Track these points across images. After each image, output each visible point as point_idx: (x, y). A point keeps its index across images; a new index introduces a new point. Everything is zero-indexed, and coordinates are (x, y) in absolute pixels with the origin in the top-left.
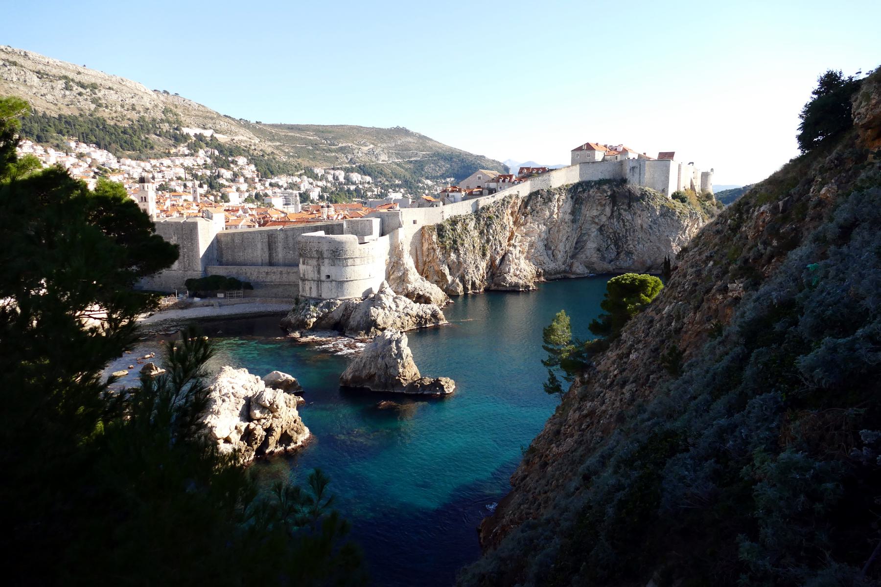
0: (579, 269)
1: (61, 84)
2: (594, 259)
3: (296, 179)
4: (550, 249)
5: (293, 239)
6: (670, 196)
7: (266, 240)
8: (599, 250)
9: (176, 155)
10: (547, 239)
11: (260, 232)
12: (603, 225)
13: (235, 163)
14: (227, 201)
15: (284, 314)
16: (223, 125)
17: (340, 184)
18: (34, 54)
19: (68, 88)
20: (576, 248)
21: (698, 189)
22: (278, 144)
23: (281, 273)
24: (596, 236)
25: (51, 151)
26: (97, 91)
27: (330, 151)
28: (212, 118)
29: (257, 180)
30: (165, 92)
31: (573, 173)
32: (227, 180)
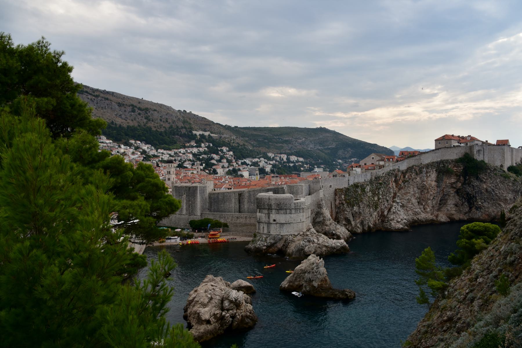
0: (443, 218)
1: (129, 109)
2: (453, 212)
3: (256, 160)
4: (422, 204)
5: (254, 197)
6: (505, 169)
7: (237, 197)
9: (188, 147)
10: (419, 198)
11: (234, 192)
12: (459, 189)
13: (222, 151)
14: (217, 173)
15: (247, 243)
17: (284, 162)
20: (440, 204)
22: (247, 139)
23: (246, 217)
24: (454, 196)
25: (122, 146)
28: (210, 125)
29: (234, 161)
30: (184, 111)
31: (437, 154)
32: (217, 161)
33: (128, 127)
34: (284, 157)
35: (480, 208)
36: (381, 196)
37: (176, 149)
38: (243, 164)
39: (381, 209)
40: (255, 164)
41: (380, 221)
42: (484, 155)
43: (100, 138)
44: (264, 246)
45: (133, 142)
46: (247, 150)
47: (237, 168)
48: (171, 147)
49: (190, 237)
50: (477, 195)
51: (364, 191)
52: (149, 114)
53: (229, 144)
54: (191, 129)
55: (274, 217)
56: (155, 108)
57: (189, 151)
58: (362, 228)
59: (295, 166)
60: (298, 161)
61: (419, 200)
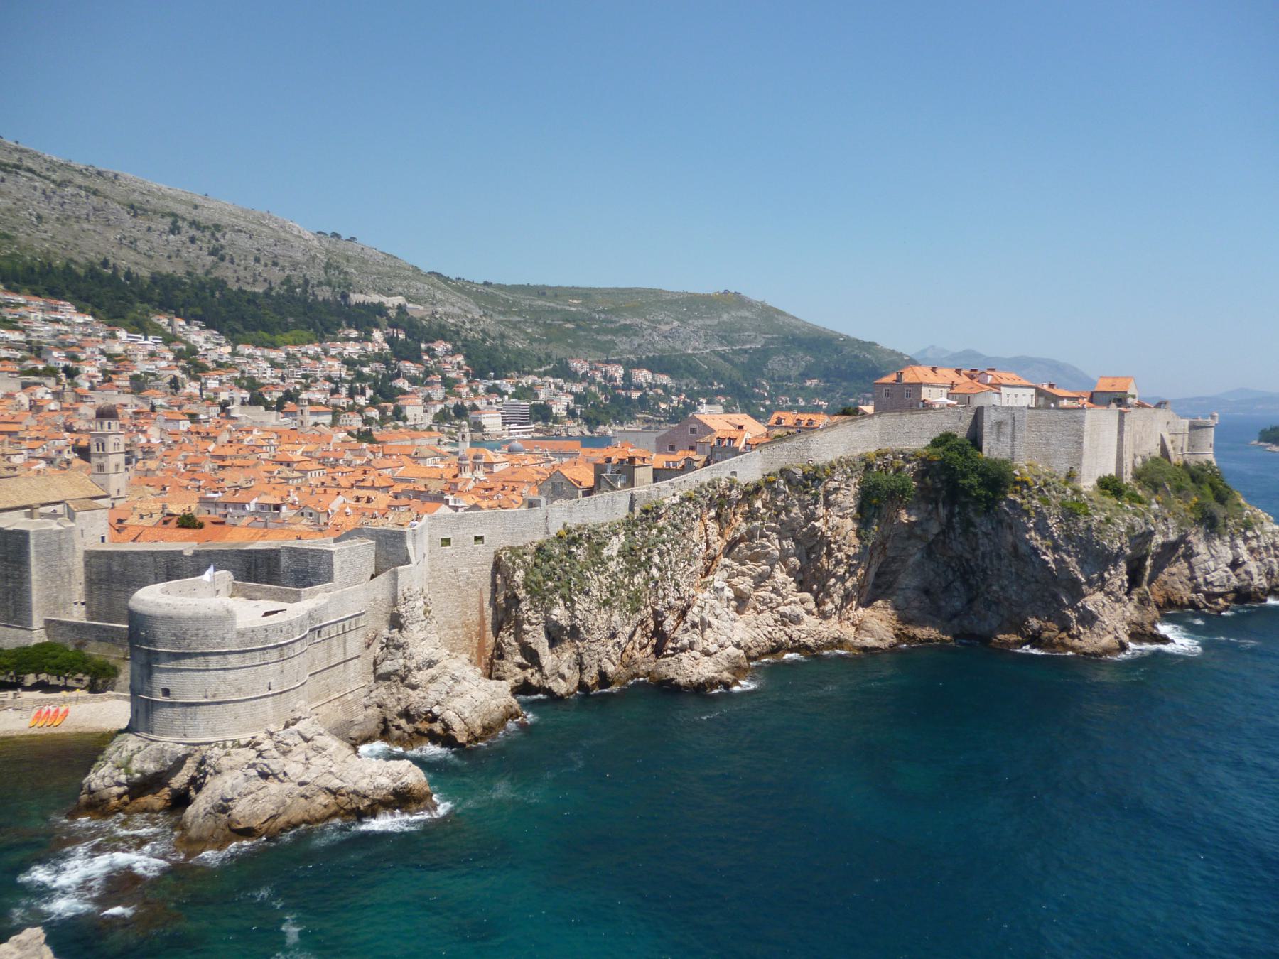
8: (927, 592)
13: (431, 352)
14: (405, 419)
16: (422, 288)
17: (616, 388)
18: (129, 175)
19: (175, 230)
21: (1176, 457)
22: (517, 319)
25: (122, 334)
26: (218, 235)
27: (606, 331)
28: (404, 278)
29: (465, 382)
30: (335, 235)
31: (865, 432)
32: (413, 381)
33: (156, 279)
34: (618, 372)
35: (997, 603)
36: (655, 572)
37: (295, 344)
38: (489, 390)
39: (656, 614)
40: (521, 393)
41: (649, 650)
42: (1013, 440)
43: (56, 309)
44: (119, 784)
45: (163, 321)
46: (507, 350)
47: (467, 404)
48: (278, 338)
50: (987, 561)
51: (598, 553)
52: (222, 242)
53: (457, 333)
54: (348, 286)
56: (243, 224)
57: (333, 352)
58: (576, 678)
59: (642, 401)
60: (651, 387)
61: (801, 577)
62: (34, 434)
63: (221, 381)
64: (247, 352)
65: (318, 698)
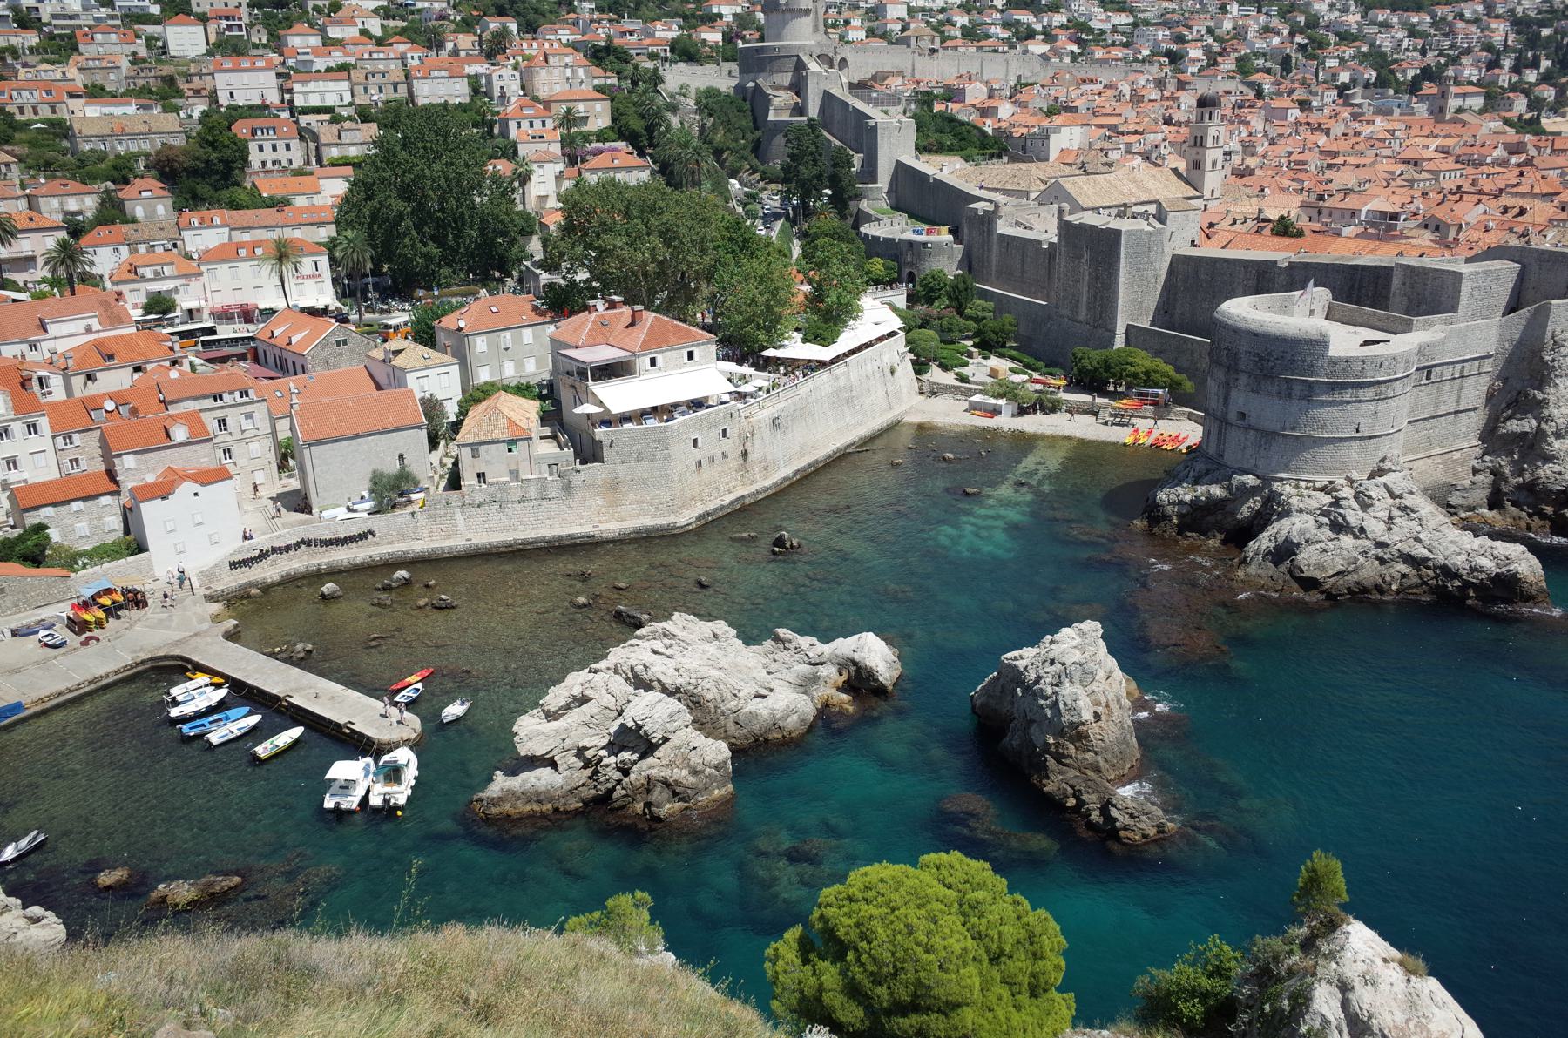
49: (1050, 408)
55: (1241, 401)
62: (1132, 128)
63: (1342, 60)
64: (1381, 18)
65: (1414, 451)
